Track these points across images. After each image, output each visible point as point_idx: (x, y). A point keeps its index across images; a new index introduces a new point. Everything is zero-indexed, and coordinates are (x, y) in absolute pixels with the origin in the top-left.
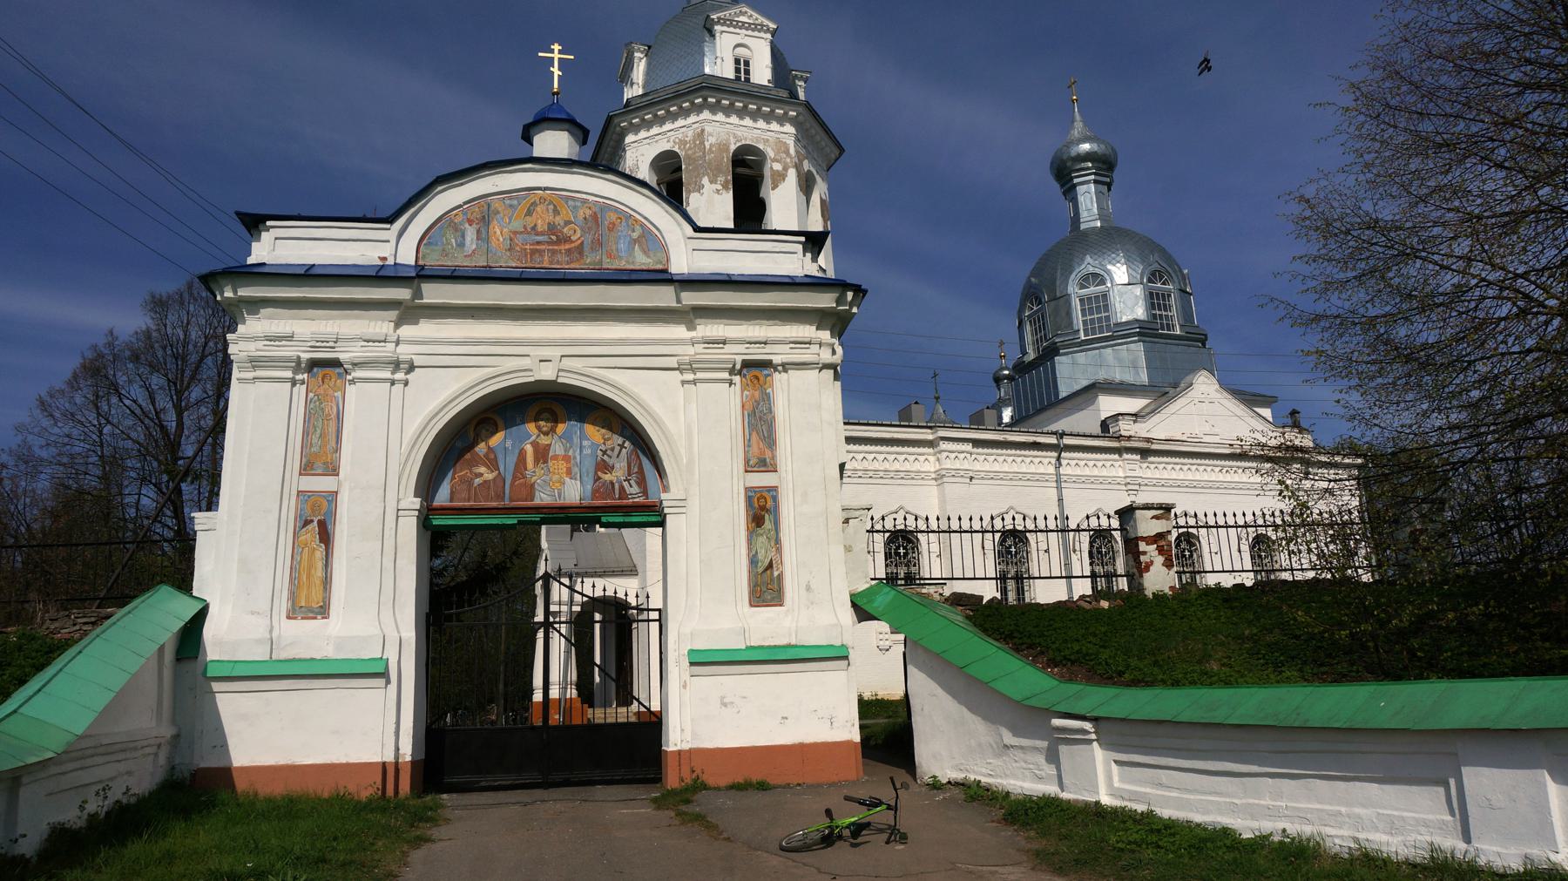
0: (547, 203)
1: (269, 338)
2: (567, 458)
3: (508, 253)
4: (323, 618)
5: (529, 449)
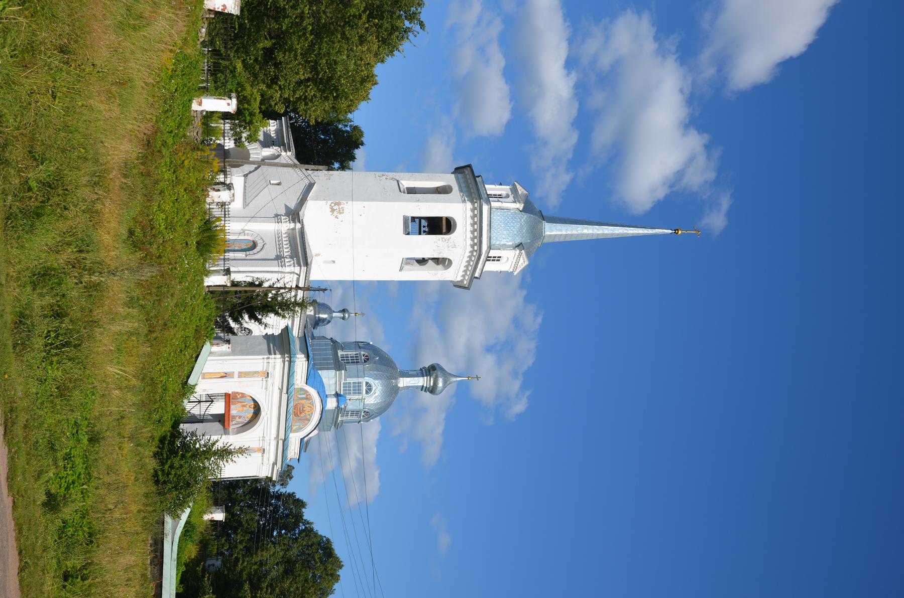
2: (242, 411)
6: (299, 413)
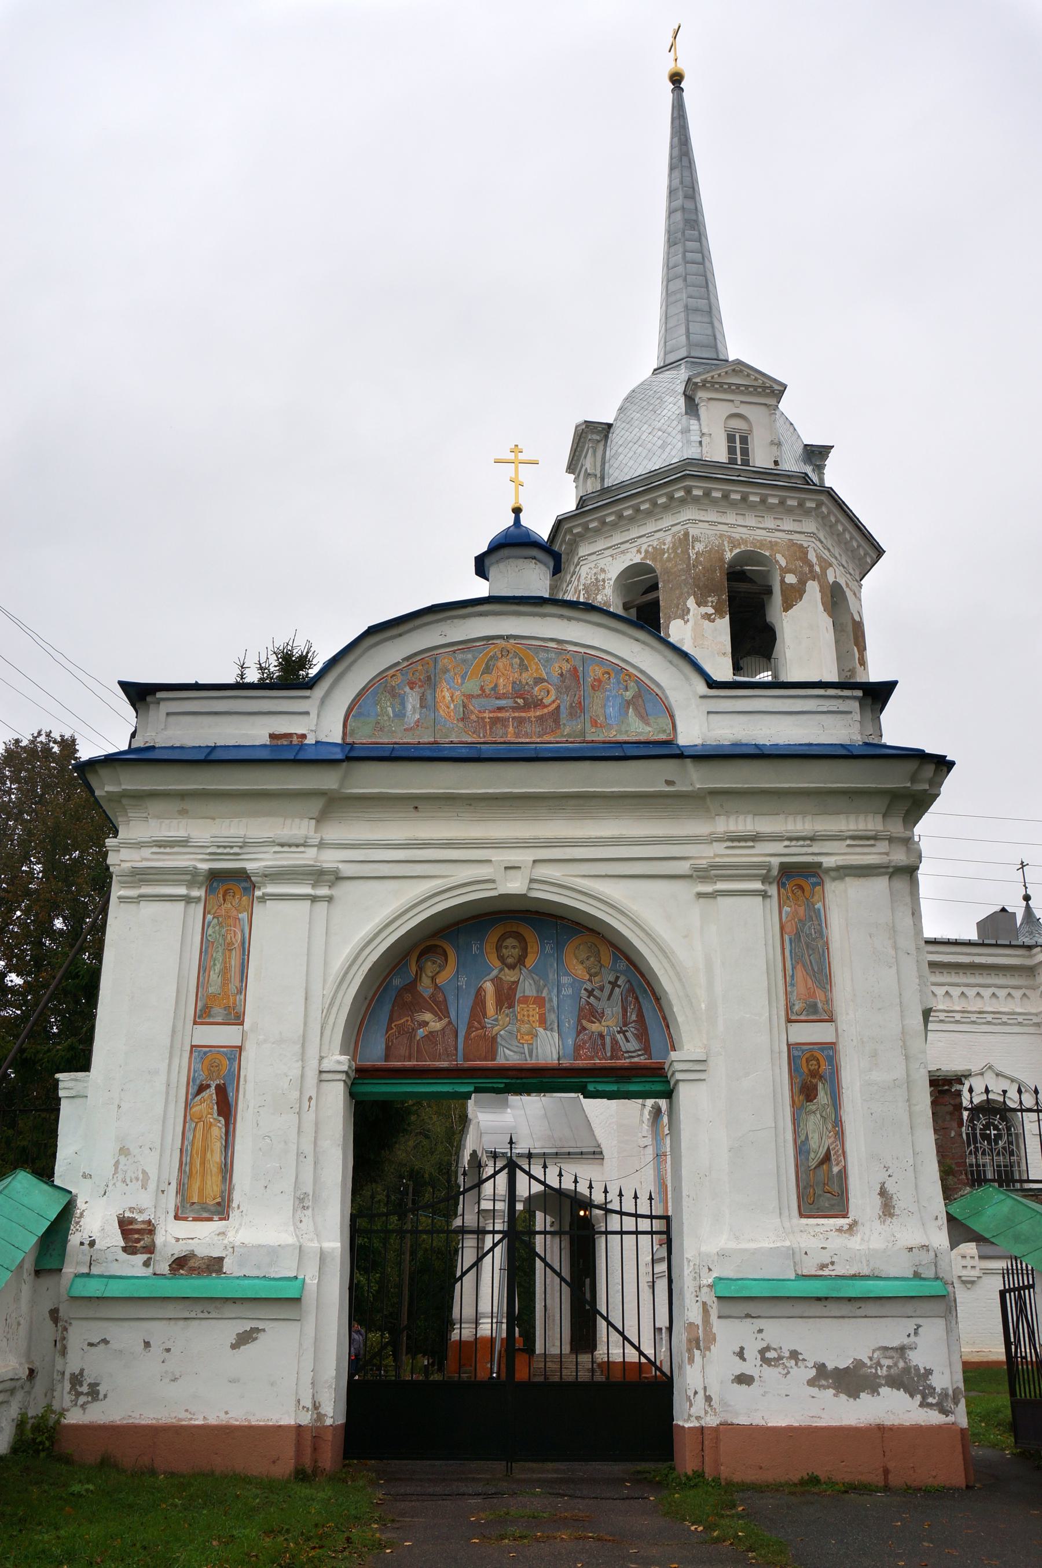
0: (511, 655)
1: (160, 844)
2: (540, 1001)
3: (461, 724)
4: (221, 1219)
5: (489, 987)
6: (533, 714)
